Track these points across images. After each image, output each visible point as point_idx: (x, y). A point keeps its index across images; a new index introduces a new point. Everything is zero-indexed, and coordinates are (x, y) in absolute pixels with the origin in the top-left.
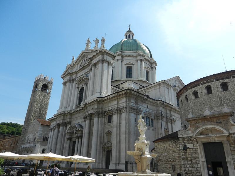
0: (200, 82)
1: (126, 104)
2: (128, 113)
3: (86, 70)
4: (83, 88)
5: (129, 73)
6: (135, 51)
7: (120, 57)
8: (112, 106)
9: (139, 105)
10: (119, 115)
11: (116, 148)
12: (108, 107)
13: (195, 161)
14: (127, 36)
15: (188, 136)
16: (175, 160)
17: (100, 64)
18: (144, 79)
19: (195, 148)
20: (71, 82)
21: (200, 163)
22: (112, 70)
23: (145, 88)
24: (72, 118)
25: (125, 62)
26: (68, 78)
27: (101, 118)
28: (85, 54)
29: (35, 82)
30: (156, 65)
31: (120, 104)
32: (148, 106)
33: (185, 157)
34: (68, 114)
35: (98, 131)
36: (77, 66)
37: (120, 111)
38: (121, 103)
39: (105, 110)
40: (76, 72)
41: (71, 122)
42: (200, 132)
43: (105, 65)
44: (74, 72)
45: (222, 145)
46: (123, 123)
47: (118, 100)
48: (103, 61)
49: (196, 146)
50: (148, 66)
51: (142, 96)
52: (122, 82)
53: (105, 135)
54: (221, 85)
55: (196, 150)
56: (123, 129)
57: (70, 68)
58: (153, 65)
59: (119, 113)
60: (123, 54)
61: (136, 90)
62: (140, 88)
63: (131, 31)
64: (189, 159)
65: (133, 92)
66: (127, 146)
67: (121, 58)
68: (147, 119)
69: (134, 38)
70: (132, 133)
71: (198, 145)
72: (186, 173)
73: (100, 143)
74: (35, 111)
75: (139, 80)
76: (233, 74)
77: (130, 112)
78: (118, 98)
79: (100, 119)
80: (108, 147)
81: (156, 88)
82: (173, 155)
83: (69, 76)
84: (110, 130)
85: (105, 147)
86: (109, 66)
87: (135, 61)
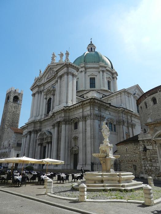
0: (158, 89)
1: (91, 112)
3: (53, 82)
4: (50, 99)
5: (93, 83)
6: (97, 63)
7: (83, 69)
8: (78, 114)
9: (103, 112)
10: (84, 122)
11: (83, 151)
12: (74, 115)
13: (154, 161)
14: (89, 49)
15: (148, 138)
16: (136, 161)
17: (66, 76)
18: (106, 88)
19: (154, 150)
20: (40, 93)
21: (158, 163)
22: (77, 81)
23: (107, 97)
25: (88, 74)
26: (36, 90)
28: (51, 67)
29: (7, 94)
30: (117, 75)
31: (85, 112)
32: (111, 112)
33: (145, 157)
35: (66, 137)
36: (44, 79)
37: (85, 118)
38: (86, 111)
39: (71, 118)
40: (44, 85)
41: (41, 129)
42: (159, 135)
43: (70, 77)
46: (88, 129)
47: (83, 109)
48: (68, 73)
49: (155, 147)
50: (109, 76)
51: (104, 104)
52: (86, 92)
53: (73, 140)
55: (155, 151)
56: (88, 134)
57: (38, 81)
58: (114, 75)
59: (84, 120)
60: (86, 66)
61: (99, 99)
62: (103, 97)
63: (92, 44)
64: (149, 159)
65: (96, 101)
66: (93, 149)
67: (84, 70)
68: (110, 125)
69: (96, 50)
70: (97, 137)
71: (156, 146)
72: (146, 171)
73: (68, 147)
74: (8, 120)
75: (102, 90)
78: (83, 107)
79: (67, 126)
80: (75, 151)
81: (117, 97)
82: (134, 156)
83: (37, 88)
84: (77, 135)
85: (72, 151)
87: (97, 72)
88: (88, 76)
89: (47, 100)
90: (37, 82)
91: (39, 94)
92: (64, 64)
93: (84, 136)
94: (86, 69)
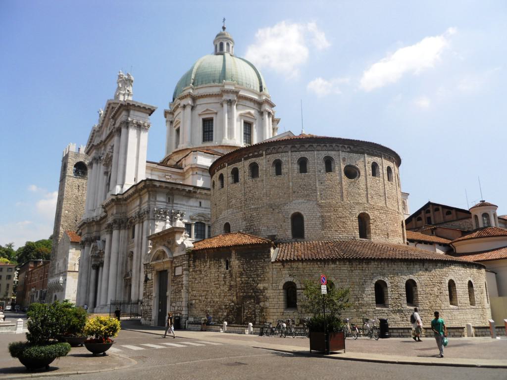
5: (209, 131)
9: (177, 204)
10: (141, 225)
14: (216, 45)
17: (123, 130)
24: (102, 229)
25: (199, 109)
32: (203, 202)
34: (94, 223)
35: (118, 253)
36: (106, 130)
40: (104, 143)
42: (156, 256)
44: (101, 143)
48: (127, 124)
51: (179, 187)
54: (232, 173)
57: (95, 135)
58: (263, 106)
59: (141, 221)
64: (148, 294)
65: (158, 184)
73: (122, 273)
75: (223, 146)
78: (140, 195)
83: (94, 151)
86: (140, 130)
87: (219, 105)
88: (200, 115)
90: (94, 138)
91: (97, 163)
92: (119, 105)
93: (139, 253)
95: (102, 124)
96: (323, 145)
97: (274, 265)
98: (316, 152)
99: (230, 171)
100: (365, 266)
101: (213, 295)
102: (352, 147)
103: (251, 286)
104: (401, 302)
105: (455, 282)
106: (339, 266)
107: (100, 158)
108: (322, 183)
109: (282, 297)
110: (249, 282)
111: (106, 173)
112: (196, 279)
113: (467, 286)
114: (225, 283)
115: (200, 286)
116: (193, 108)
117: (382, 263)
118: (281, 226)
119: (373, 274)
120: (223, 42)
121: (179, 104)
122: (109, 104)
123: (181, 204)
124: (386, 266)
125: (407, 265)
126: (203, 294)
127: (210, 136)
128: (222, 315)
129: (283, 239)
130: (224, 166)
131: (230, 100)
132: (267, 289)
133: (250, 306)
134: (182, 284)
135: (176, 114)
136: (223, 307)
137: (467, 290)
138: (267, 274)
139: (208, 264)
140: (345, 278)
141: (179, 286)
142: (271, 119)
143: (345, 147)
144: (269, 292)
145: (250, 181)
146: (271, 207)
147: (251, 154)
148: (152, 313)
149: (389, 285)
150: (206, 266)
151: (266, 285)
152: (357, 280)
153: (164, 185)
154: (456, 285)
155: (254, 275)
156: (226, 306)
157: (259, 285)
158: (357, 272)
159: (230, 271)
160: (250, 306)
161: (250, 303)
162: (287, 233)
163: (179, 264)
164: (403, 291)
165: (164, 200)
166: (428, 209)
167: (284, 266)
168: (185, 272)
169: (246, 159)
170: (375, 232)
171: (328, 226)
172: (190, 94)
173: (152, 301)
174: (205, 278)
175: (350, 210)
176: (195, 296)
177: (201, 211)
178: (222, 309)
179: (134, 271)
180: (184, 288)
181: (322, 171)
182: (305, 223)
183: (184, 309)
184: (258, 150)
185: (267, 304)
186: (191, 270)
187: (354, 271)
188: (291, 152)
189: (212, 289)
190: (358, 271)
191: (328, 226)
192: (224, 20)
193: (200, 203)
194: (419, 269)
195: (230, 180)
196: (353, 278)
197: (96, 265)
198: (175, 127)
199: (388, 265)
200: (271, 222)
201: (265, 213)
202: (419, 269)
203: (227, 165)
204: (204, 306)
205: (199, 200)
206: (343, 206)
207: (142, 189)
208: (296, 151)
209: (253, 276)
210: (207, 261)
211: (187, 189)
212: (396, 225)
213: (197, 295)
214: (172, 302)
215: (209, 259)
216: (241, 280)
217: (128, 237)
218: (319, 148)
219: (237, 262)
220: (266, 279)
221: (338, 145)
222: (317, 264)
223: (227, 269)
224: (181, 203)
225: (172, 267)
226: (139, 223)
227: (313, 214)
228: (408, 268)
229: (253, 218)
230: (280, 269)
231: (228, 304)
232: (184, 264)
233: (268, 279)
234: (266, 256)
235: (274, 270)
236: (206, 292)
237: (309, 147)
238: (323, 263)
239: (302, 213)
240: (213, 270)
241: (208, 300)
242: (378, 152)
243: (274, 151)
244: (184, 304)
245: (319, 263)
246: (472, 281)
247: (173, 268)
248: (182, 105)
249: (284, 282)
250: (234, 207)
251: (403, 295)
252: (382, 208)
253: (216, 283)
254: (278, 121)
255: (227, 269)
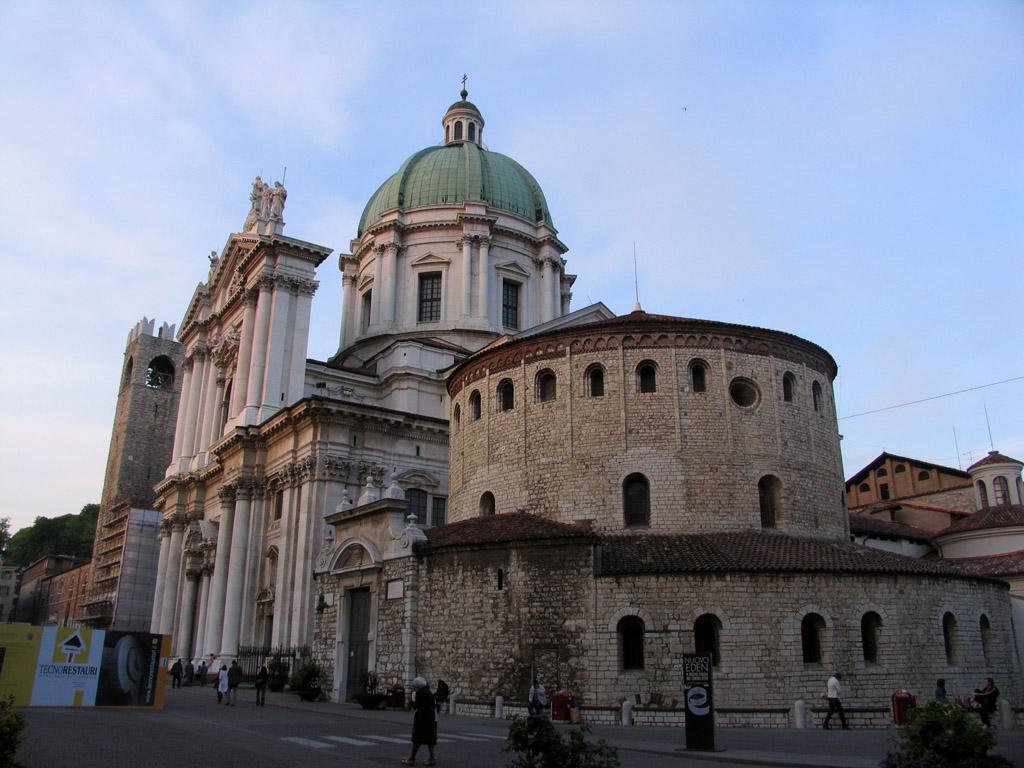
1: (314, 450)
2: (308, 484)
5: (432, 300)
9: (372, 450)
10: (296, 490)
20: (206, 356)
24: (207, 498)
25: (414, 254)
27: (258, 502)
28: (240, 245)
33: (318, 630)
35: (246, 549)
36: (224, 294)
43: (281, 296)
44: (211, 320)
45: (369, 597)
48: (270, 282)
50: (512, 258)
51: (376, 415)
57: (200, 304)
59: (296, 484)
61: (434, 377)
63: (473, 107)
64: (324, 636)
65: (334, 408)
73: (253, 590)
76: (528, 352)
77: (325, 481)
87: (453, 248)
89: (224, 388)
92: (257, 244)
94: (404, 232)
95: (217, 281)
96: (688, 335)
97: (599, 581)
98: (673, 350)
99: (494, 385)
100: (782, 583)
101: (469, 641)
102: (744, 341)
103: (551, 624)
104: (854, 658)
105: (956, 618)
106: (731, 585)
107: (209, 350)
108: (686, 414)
109: (616, 647)
110: (547, 615)
111: (221, 382)
112: (433, 607)
113: (979, 625)
114: (496, 617)
115: (443, 622)
116: (400, 252)
117: (817, 579)
118: (604, 501)
119: (797, 600)
120: (462, 120)
121: (373, 244)
122: (234, 242)
123: (379, 451)
124: (824, 585)
125: (864, 582)
126: (448, 639)
127: (434, 309)
128: (488, 683)
129: (608, 528)
130: (483, 376)
131: (477, 237)
132: (583, 631)
133: (549, 665)
134: (403, 618)
135: (364, 262)
136: (492, 666)
137: (979, 634)
138: (583, 600)
139: (460, 576)
140: (744, 609)
141: (397, 621)
142: (558, 275)
143: (731, 342)
144: (587, 636)
145: (537, 408)
146: (583, 462)
147: (541, 352)
148: (335, 674)
149: (829, 624)
150: (456, 580)
151: (582, 622)
152: (768, 613)
153: (346, 410)
154: (958, 624)
155: (557, 601)
156: (498, 663)
157: (567, 623)
158: (767, 596)
159: (506, 593)
160: (549, 665)
161: (548, 660)
162: (614, 516)
163: (397, 577)
164: (857, 636)
165: (344, 440)
166: (882, 467)
167: (619, 584)
168: (409, 593)
169: (529, 361)
170: (792, 514)
171: (698, 501)
172: (395, 224)
173: (335, 651)
174: (453, 606)
175: (743, 471)
176: (431, 643)
177: (418, 466)
178: (489, 671)
179: (279, 587)
180: (408, 625)
181: (687, 389)
182: (653, 496)
183: (407, 668)
184: (555, 343)
185: (585, 661)
186: (423, 588)
187: (761, 595)
188: (624, 349)
189: (466, 628)
190: (770, 595)
191: (698, 501)
192: (465, 78)
193: (418, 448)
194: (887, 591)
195: (495, 403)
196: (759, 608)
197: (195, 571)
198: (360, 290)
199: (827, 582)
200: (582, 494)
201: (571, 473)
202: (887, 591)
203: (487, 373)
204: (451, 665)
205: (415, 443)
206: (729, 460)
207: (302, 417)
208: (633, 348)
209: (553, 604)
210: (458, 570)
211: (393, 419)
212: (831, 500)
213: (434, 640)
214: (378, 655)
215: (461, 567)
216: (530, 612)
217: (267, 516)
218: (682, 342)
219: (522, 574)
220: (583, 609)
221: (718, 336)
222: (687, 580)
223: (500, 587)
224: (380, 448)
225: (379, 583)
226: (292, 488)
227: (670, 478)
228: (865, 588)
229: (545, 484)
230: (612, 590)
231: (501, 661)
232: (408, 576)
233: (587, 610)
234: (582, 563)
235: (600, 591)
236: (454, 635)
237: (660, 338)
238: (698, 579)
239: (647, 475)
240: (471, 590)
241: (460, 651)
242: (796, 351)
243: (587, 346)
244: (407, 658)
245: (690, 578)
246: (987, 615)
247: (383, 584)
248: (378, 244)
249: (618, 616)
250: (504, 459)
251: (858, 645)
252: (805, 466)
253: (477, 615)
254: (571, 280)
255: (500, 587)
